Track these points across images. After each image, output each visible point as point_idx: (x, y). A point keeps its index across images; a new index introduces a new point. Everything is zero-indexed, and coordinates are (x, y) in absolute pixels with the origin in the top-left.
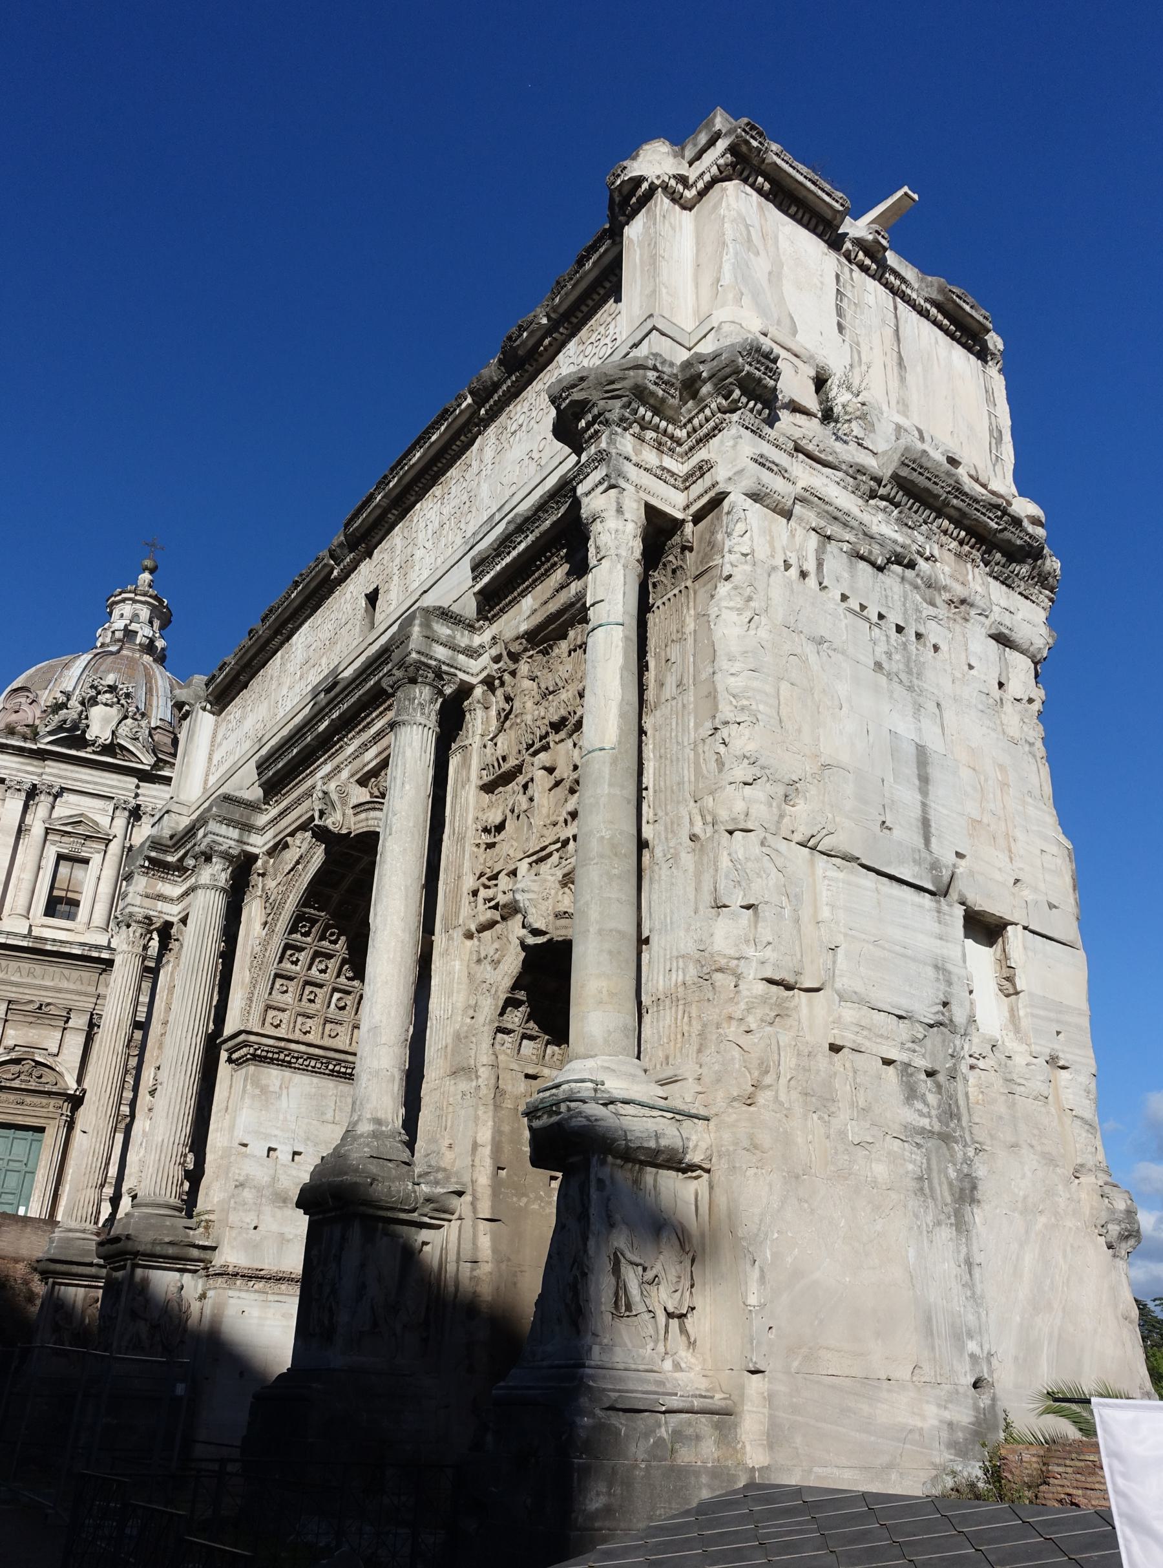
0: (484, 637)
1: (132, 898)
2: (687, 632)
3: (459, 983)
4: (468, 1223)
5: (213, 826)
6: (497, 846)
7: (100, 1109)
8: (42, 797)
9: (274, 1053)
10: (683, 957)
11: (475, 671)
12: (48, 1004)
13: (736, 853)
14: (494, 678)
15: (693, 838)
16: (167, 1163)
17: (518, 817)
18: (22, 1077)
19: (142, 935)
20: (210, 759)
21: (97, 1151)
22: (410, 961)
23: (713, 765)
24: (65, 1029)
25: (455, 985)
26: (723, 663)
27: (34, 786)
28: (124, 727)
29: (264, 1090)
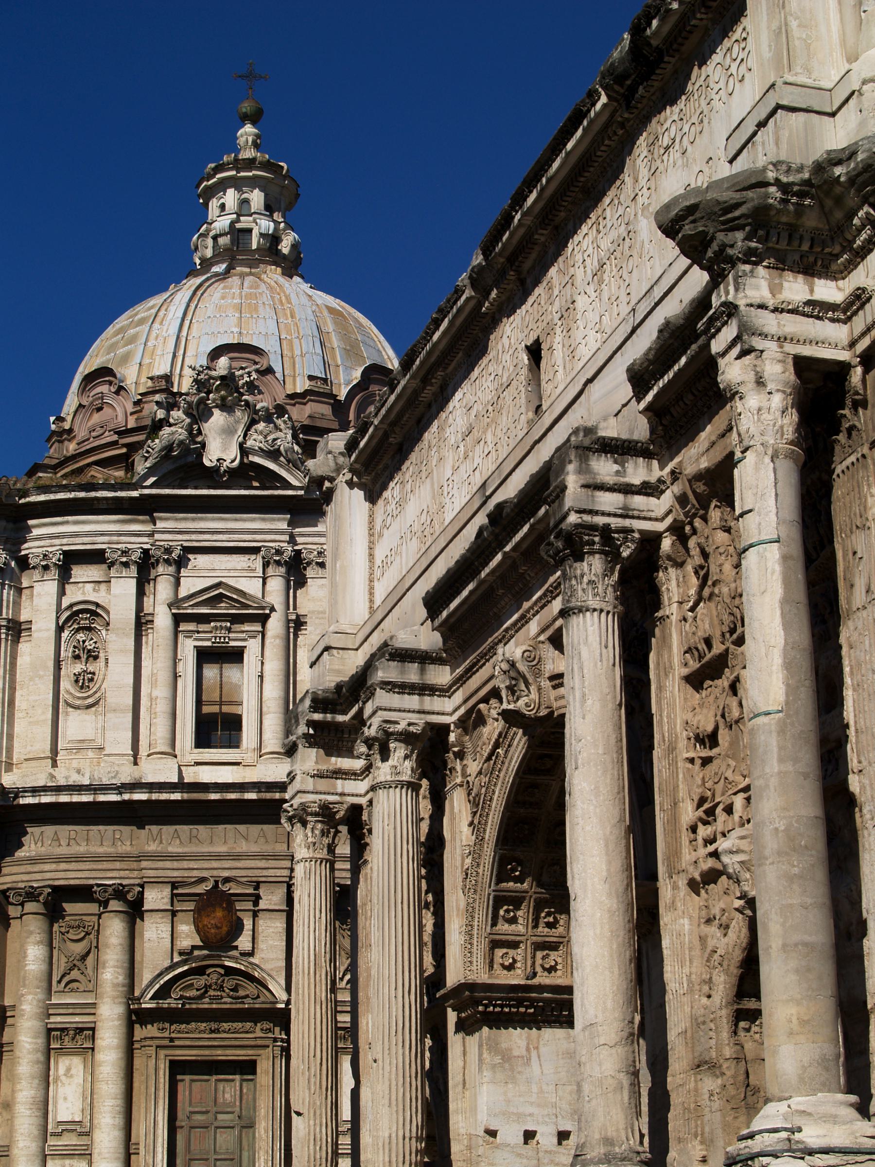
1: (302, 782)
2: (870, 518)
3: (690, 949)
5: (382, 698)
6: (715, 762)
7: (313, 1080)
8: (161, 569)
9: (510, 1006)
11: (659, 512)
12: (227, 880)
18: (211, 993)
19: (322, 831)
21: (318, 1136)
22: (622, 933)
24: (255, 914)
27: (146, 552)
28: (255, 436)
29: (507, 1057)
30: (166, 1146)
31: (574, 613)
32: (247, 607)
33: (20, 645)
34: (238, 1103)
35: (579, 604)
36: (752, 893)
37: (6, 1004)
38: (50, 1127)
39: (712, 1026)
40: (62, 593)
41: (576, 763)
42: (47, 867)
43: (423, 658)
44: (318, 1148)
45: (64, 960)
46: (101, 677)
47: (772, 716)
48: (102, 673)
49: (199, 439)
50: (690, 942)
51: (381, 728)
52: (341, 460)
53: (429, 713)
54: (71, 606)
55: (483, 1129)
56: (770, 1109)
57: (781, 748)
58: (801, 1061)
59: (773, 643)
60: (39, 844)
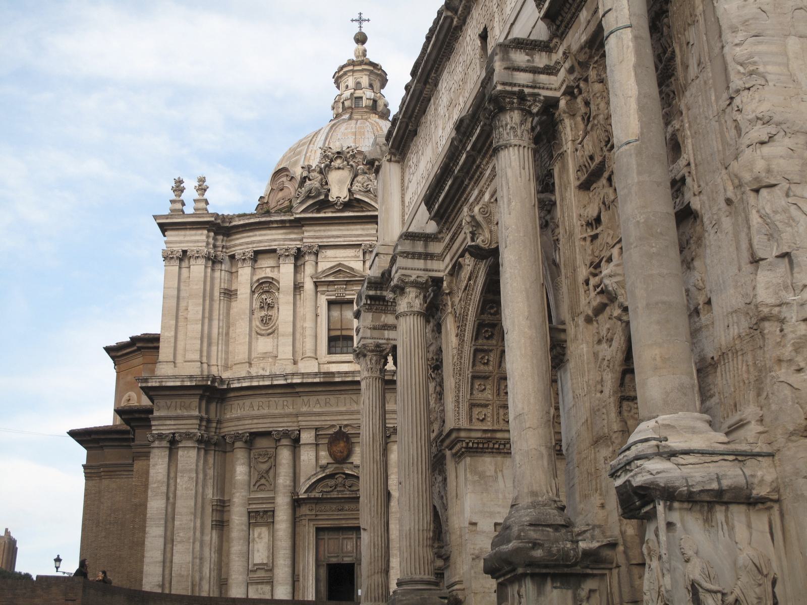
0: (558, 56)
1: (364, 332)
2: (698, 14)
3: (588, 363)
4: (623, 569)
5: (401, 262)
7: (372, 508)
8: (307, 258)
10: (736, 311)
11: (556, 85)
12: (346, 426)
13: (764, 208)
14: (572, 87)
15: (729, 202)
16: (417, 548)
17: (609, 207)
18: (338, 489)
20: (403, 202)
21: (376, 543)
23: (733, 132)
25: (586, 366)
26: (728, 36)
27: (299, 249)
28: (357, 184)
29: (482, 476)
30: (314, 576)
31: (502, 149)
32: (355, 276)
33: (232, 303)
34: (355, 551)
35: (505, 142)
36: (626, 304)
37: (225, 499)
38: (250, 567)
39: (604, 411)
40: (253, 274)
41: (506, 243)
42: (247, 422)
43: (427, 238)
44: (376, 550)
45: (256, 473)
46: (276, 318)
47: (631, 144)
48: (276, 316)
49: (326, 187)
50: (588, 359)
51: (400, 279)
52: (384, 148)
53: (430, 271)
54: (258, 280)
55: (468, 522)
56: (643, 426)
57: (638, 165)
58: (665, 388)
59: (630, 94)
60: (242, 410)
